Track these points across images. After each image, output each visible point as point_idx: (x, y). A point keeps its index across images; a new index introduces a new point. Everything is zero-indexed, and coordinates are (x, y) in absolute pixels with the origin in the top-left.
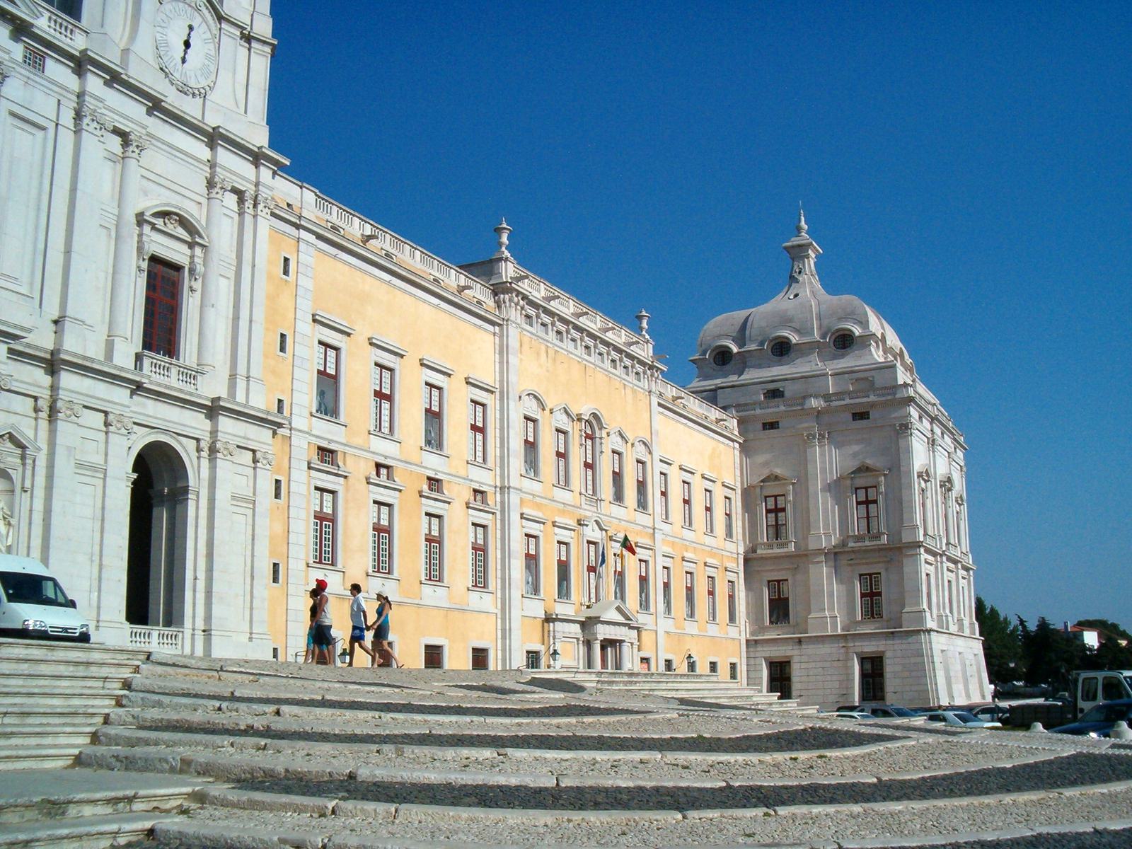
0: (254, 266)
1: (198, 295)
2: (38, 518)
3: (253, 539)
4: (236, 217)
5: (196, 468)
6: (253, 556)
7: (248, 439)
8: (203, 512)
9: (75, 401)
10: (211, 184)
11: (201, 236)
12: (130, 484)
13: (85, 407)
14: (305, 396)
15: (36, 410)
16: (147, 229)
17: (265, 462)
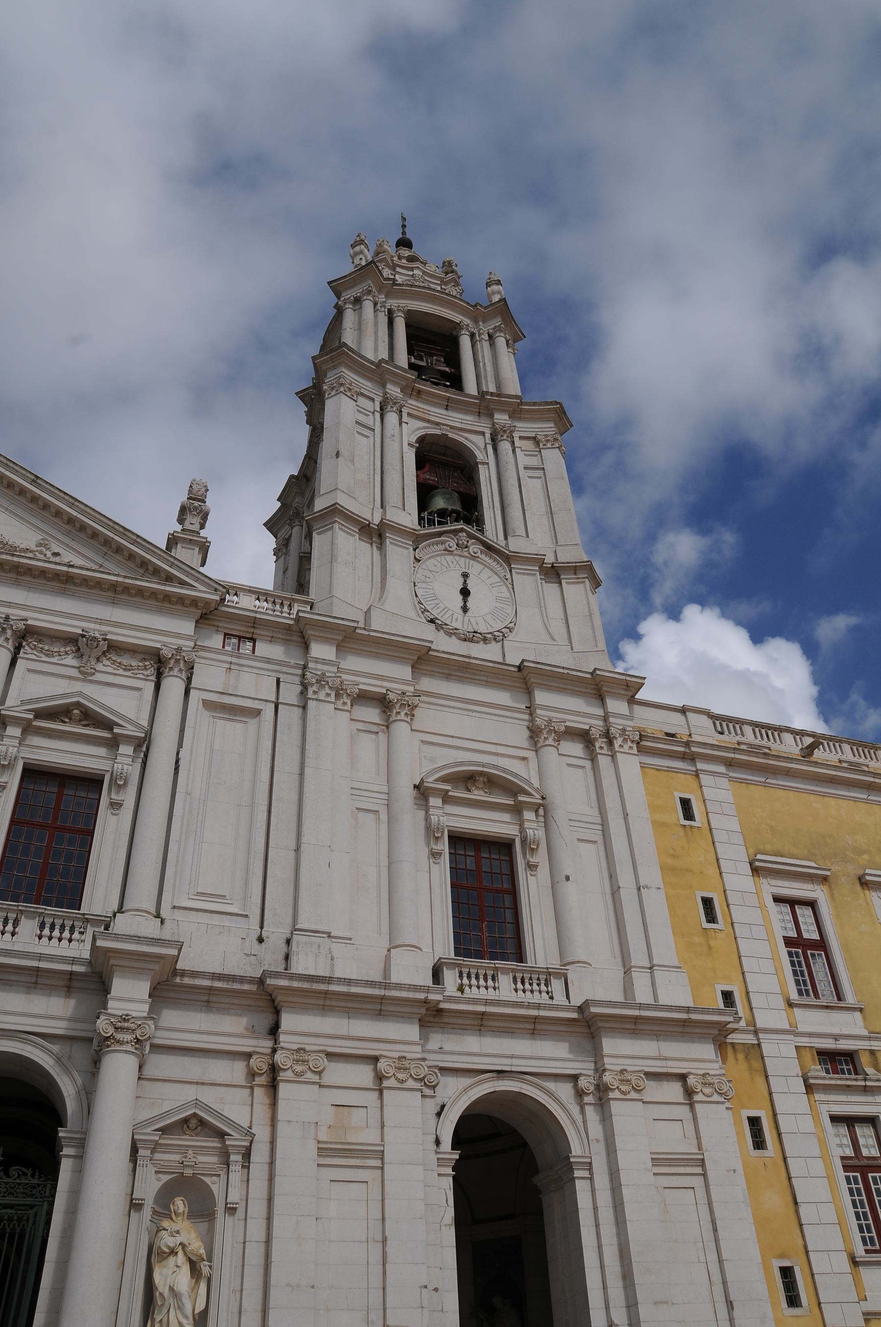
0: (626, 815)
1: (544, 870)
2: (255, 1253)
3: (715, 1230)
4: (588, 764)
6: (721, 1261)
8: (604, 1198)
9: (308, 1048)
10: (534, 733)
11: (528, 794)
12: (449, 1171)
13: (331, 1056)
14: (767, 978)
15: (252, 1075)
16: (435, 802)
17: (708, 1090)
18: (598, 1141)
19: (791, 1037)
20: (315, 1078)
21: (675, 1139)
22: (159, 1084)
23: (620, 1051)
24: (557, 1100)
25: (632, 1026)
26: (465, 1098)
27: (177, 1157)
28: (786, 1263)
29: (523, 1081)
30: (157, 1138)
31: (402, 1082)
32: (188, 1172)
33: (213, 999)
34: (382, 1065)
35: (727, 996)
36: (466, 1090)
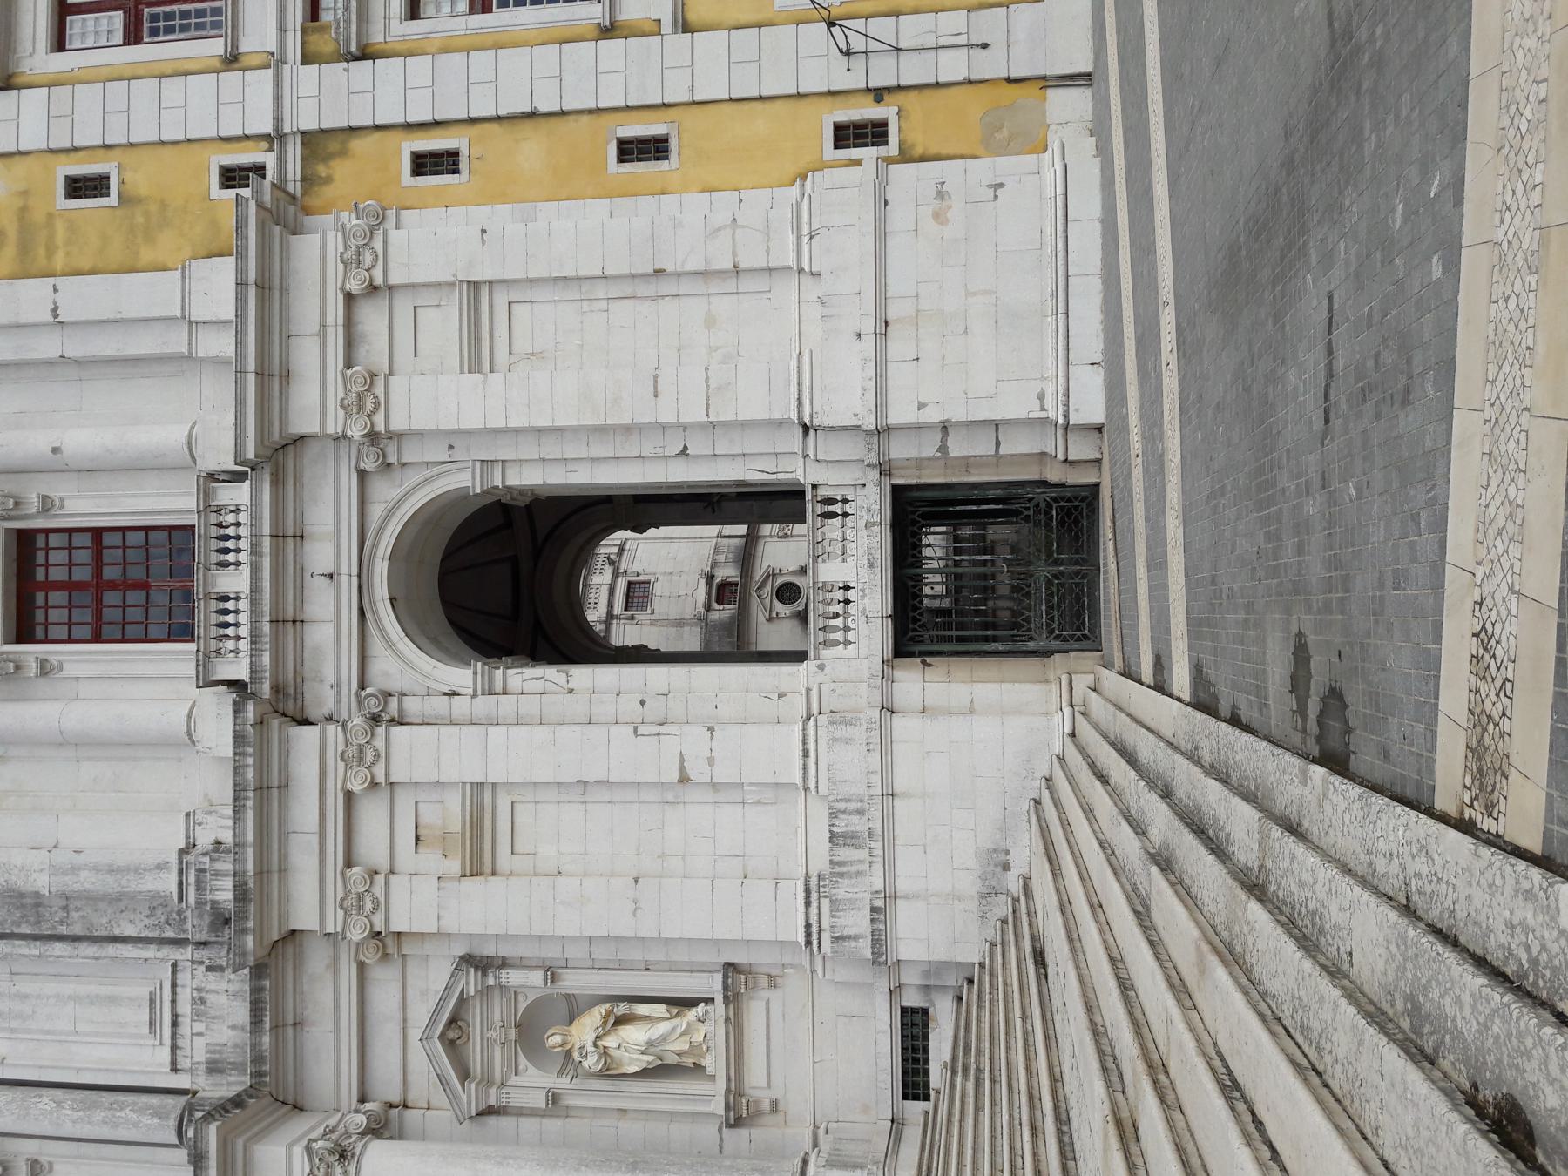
5: (427, 473)
7: (323, 326)
9: (340, 895)
12: (499, 673)
18: (451, 447)
19: (286, 68)
20: (380, 879)
21: (442, 325)
22: (411, 1078)
23: (313, 404)
24: (398, 504)
25: (276, 381)
26: (401, 646)
27: (497, 1049)
28: (613, 150)
29: (372, 557)
30: (473, 1086)
31: (377, 756)
32: (513, 1034)
33: (290, 1020)
34: (356, 786)
35: (232, 177)
36: (390, 645)
